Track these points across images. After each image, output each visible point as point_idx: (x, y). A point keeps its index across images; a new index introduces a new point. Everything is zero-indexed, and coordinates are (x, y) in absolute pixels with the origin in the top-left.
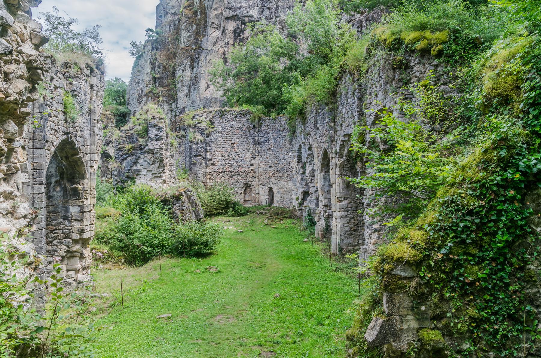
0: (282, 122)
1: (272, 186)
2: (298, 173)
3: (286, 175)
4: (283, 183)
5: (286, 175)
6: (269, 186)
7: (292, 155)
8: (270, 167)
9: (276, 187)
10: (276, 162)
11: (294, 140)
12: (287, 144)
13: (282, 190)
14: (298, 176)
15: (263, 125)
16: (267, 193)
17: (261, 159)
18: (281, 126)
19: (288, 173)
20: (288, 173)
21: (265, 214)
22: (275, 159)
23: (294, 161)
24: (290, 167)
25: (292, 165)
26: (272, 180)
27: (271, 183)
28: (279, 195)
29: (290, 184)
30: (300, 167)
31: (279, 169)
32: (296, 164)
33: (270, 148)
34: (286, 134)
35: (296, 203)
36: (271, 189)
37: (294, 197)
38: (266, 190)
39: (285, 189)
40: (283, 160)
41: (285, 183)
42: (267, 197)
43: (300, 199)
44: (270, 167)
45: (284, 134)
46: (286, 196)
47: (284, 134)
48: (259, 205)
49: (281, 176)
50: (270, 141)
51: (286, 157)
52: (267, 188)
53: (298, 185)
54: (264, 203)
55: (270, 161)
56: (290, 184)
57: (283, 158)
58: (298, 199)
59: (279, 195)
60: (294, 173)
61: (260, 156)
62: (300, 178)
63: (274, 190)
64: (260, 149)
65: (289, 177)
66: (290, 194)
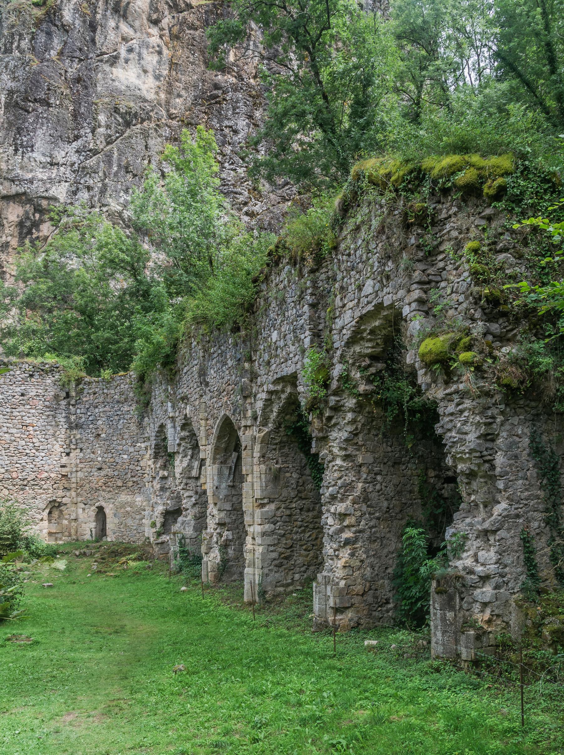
0: (122, 386)
1: (103, 504)
2: (154, 478)
3: (130, 484)
4: (124, 497)
5: (130, 484)
6: (97, 504)
7: (143, 445)
8: (100, 469)
9: (111, 506)
10: (112, 460)
11: (146, 419)
12: (133, 427)
13: (122, 510)
14: (155, 483)
15: (86, 391)
16: (93, 518)
17: (82, 455)
18: (122, 394)
19: (135, 479)
20: (135, 479)
21: (92, 555)
22: (110, 455)
23: (147, 456)
24: (139, 468)
25: (142, 463)
26: (103, 493)
27: (101, 499)
28: (116, 521)
29: (138, 499)
30: (158, 466)
31: (116, 473)
32: (150, 463)
33: (99, 435)
34: (131, 409)
35: (150, 532)
36: (101, 510)
37: (147, 522)
38: (92, 512)
39: (128, 509)
40: (125, 457)
41: (129, 498)
42: (93, 525)
43: (158, 525)
44: (100, 469)
45: (126, 408)
46: (130, 522)
47: (126, 408)
48: (77, 540)
49: (120, 483)
50: (100, 422)
51: (131, 449)
52: (94, 508)
53: (154, 499)
54: (87, 537)
55: (100, 459)
56: (139, 499)
57: (125, 452)
58: (154, 525)
59: (116, 521)
60: (147, 478)
61: (78, 450)
62: (159, 486)
63: (107, 511)
64: (78, 436)
65: (137, 486)
66: (138, 517)
